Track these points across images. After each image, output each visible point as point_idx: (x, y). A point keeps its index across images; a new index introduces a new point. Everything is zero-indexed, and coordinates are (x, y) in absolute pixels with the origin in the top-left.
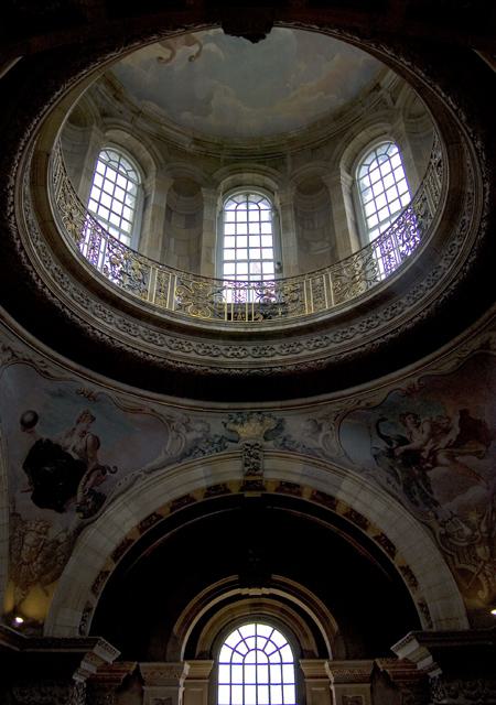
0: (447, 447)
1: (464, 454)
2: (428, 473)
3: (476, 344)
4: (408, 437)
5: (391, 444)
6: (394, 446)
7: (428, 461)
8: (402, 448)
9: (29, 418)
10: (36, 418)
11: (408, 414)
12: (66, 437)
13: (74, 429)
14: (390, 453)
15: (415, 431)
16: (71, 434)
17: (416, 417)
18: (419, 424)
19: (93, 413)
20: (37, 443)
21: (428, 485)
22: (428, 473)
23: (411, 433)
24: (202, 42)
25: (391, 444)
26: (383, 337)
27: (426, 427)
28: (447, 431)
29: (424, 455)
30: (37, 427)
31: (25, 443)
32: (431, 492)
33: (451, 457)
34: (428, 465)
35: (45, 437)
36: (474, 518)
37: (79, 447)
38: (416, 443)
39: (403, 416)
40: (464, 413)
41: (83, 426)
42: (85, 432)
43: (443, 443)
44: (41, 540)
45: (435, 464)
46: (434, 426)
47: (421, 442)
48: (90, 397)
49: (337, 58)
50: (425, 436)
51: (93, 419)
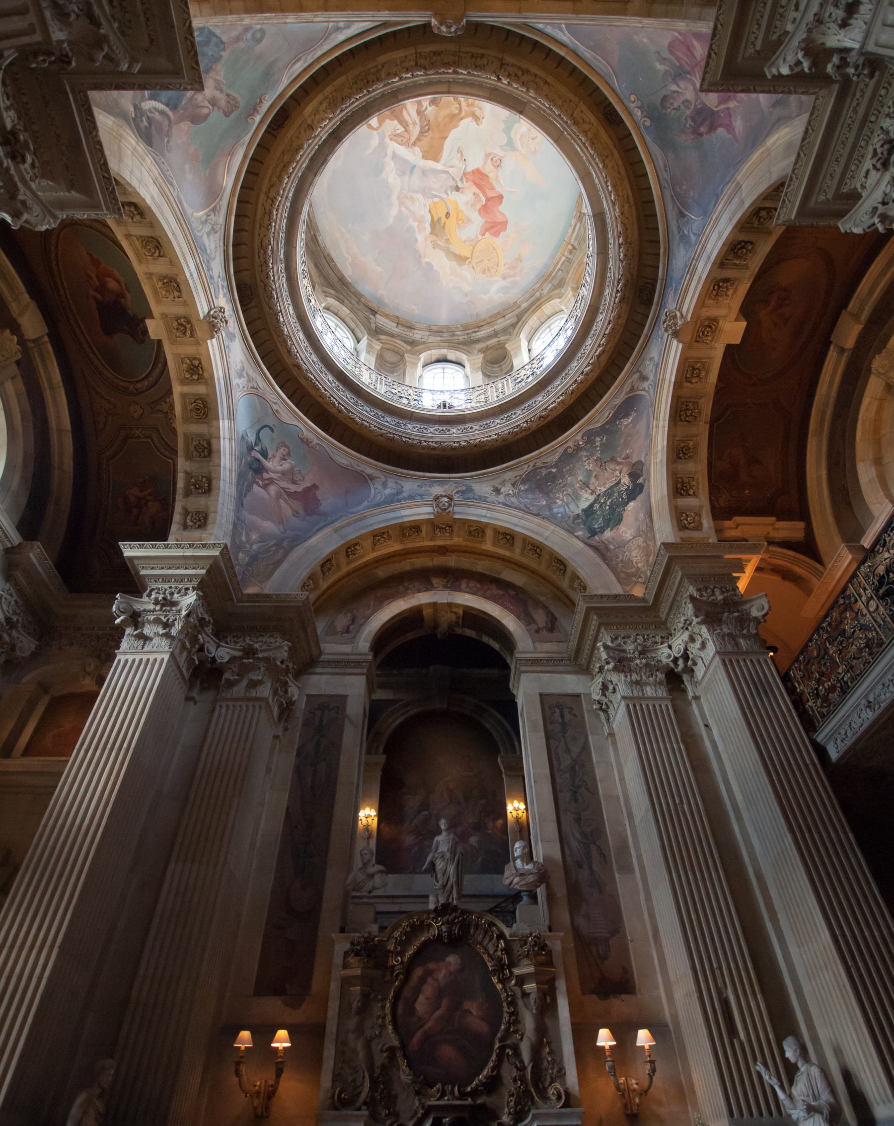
0: (283, 489)
1: (287, 502)
2: (255, 486)
3: (369, 471)
4: (270, 456)
5: (256, 444)
6: (256, 448)
7: (263, 480)
8: (259, 456)
11: (288, 448)
13: (221, 91)
14: (251, 448)
15: (277, 459)
17: (289, 454)
18: (285, 460)
21: (248, 490)
22: (255, 486)
23: (274, 456)
24: (380, 130)
25: (256, 444)
26: (339, 403)
27: (286, 466)
28: (294, 482)
29: (265, 475)
32: (245, 496)
33: (279, 496)
34: (261, 483)
36: (254, 537)
38: (268, 464)
39: (284, 445)
40: (315, 486)
43: (283, 484)
45: (265, 487)
46: (291, 471)
47: (272, 468)
49: (379, 269)
50: (279, 468)
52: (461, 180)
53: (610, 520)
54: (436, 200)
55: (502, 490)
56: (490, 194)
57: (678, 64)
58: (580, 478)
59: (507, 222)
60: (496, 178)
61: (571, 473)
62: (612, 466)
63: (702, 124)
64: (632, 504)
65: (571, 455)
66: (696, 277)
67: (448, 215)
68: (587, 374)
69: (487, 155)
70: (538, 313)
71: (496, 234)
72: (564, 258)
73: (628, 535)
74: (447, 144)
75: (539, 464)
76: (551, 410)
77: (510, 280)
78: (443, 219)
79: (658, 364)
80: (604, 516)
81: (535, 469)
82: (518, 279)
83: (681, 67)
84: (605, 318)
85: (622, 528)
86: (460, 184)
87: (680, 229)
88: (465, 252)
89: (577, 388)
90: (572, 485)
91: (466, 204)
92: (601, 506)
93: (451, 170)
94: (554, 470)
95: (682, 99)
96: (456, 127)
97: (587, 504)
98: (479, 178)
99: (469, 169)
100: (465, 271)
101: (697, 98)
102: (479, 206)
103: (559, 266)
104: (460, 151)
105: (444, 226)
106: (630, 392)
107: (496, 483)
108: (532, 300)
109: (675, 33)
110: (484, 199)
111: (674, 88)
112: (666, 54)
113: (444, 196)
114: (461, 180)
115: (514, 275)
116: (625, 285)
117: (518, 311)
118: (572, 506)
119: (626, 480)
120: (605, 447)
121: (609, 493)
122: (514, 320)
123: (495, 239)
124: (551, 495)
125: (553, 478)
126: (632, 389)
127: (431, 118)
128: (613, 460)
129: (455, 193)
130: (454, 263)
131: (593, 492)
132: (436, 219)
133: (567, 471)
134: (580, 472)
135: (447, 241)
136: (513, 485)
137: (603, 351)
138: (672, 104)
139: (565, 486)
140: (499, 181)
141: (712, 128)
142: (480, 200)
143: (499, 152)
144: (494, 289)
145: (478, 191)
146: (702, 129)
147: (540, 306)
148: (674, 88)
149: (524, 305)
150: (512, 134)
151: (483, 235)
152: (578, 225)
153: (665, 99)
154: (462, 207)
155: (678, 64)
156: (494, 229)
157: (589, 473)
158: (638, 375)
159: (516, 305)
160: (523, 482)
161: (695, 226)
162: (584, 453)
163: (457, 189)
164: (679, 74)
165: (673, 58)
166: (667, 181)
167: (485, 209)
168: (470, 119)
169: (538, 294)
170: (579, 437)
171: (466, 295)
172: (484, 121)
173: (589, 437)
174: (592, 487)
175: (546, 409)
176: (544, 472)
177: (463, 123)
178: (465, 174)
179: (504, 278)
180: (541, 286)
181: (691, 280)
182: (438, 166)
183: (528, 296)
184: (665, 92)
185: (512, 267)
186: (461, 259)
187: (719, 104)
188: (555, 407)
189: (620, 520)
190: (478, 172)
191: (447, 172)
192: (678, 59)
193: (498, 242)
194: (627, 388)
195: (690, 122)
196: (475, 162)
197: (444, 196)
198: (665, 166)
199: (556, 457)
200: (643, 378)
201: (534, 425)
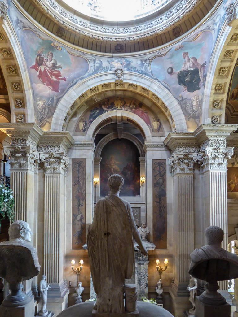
9: (170, 70)
10: (172, 69)
12: (185, 66)
16: (185, 64)
19: (186, 51)
20: (178, 75)
30: (174, 71)
31: (175, 77)
35: (179, 71)
37: (191, 65)
41: (186, 58)
42: (189, 59)
44: (198, 101)
48: (180, 48)
51: (188, 53)
57: (55, 69)
83: (54, 69)
95: (49, 61)
101: (46, 65)
109: (61, 78)
111: (52, 62)
112: (60, 69)
138: (50, 56)
148: (52, 62)
153: (52, 55)
155: (55, 69)
164: (54, 66)
165: (57, 70)
166: (36, 31)
184: (53, 58)
187: (40, 70)
192: (57, 71)
195: (43, 56)
198: (40, 36)
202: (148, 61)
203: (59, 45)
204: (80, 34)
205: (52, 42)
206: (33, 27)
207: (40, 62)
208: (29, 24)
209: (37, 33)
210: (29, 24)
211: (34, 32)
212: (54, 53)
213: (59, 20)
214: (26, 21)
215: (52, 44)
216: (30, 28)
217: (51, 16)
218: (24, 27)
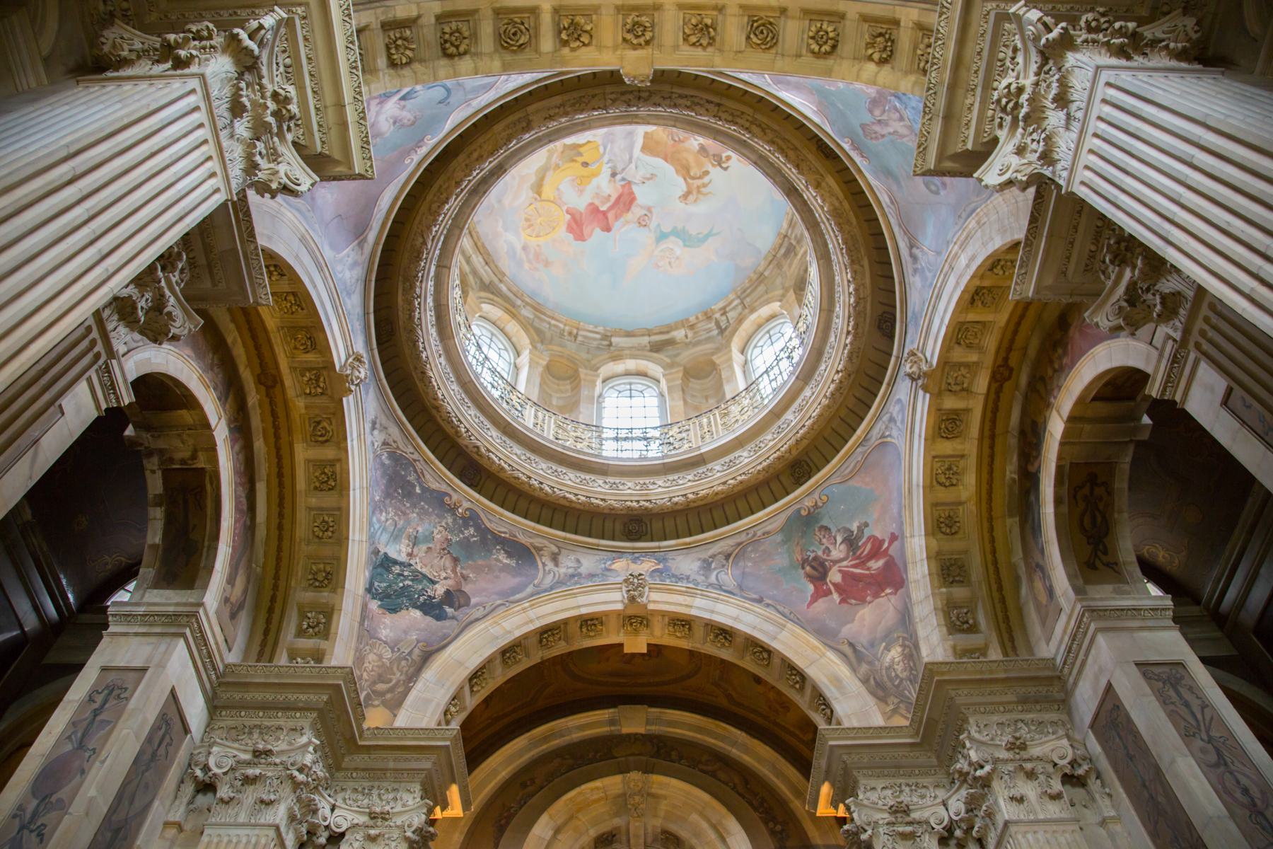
52: (623, 179)
53: (388, 596)
54: (601, 149)
55: (376, 432)
56: (611, 215)
58: (420, 529)
59: (584, 240)
60: (628, 222)
61: (423, 514)
62: (447, 562)
63: (813, 568)
64: (417, 614)
65: (442, 504)
66: (688, 600)
67: (585, 164)
68: (541, 489)
69: (649, 209)
70: (507, 317)
71: (570, 229)
72: (561, 326)
73: (384, 633)
74: (659, 162)
75: (419, 466)
76: (489, 458)
77: (523, 256)
78: (580, 159)
79: (580, 575)
80: (390, 586)
81: (411, 464)
82: (526, 266)
84: (606, 494)
85: (388, 619)
86: (618, 177)
87: (713, 556)
88: (548, 191)
89: (523, 483)
90: (408, 522)
91: (598, 187)
92: (399, 575)
93: (633, 166)
94: (418, 490)
96: (677, 172)
97: (393, 555)
98: (625, 201)
99: (635, 189)
100: (526, 194)
102: (597, 202)
103: (553, 322)
104: (653, 176)
105: (573, 161)
106: (535, 548)
107: (383, 419)
108: (511, 295)
110: (604, 208)
113: (606, 158)
114: (623, 179)
115: (529, 262)
116: (646, 509)
117: (496, 280)
118: (385, 537)
119: (440, 590)
120: (466, 545)
121: (418, 577)
122: (487, 282)
123: (563, 228)
124: (388, 501)
125: (409, 494)
126: (539, 549)
127: (686, 145)
128: (456, 560)
129: (609, 172)
130: (533, 179)
131: (410, 555)
132: (582, 150)
133: (423, 508)
134: (427, 525)
135: (557, 167)
136: (385, 443)
137: (571, 501)
139: (404, 513)
140: (624, 225)
141: (811, 578)
142: (603, 203)
143: (653, 225)
144: (510, 237)
145: (613, 199)
146: (808, 568)
147: (514, 316)
149: (503, 288)
150: (672, 238)
151: (568, 212)
152: (598, 336)
154: (595, 181)
156: (574, 226)
157: (429, 538)
158: (556, 550)
159: (501, 275)
160: (392, 455)
161: (722, 576)
162: (450, 520)
163: (614, 175)
166: (754, 535)
167: (594, 210)
168: (685, 189)
169: (519, 302)
170: (466, 505)
171: (499, 201)
172: (682, 205)
173: (470, 518)
174: (416, 550)
175: (488, 450)
176: (412, 478)
177: (681, 180)
178: (629, 183)
179: (525, 248)
180: (527, 304)
181: (681, 593)
182: (637, 151)
183: (514, 289)
185: (537, 256)
186: (538, 188)
188: (494, 462)
189: (394, 610)
190: (632, 199)
191: (630, 161)
193: (562, 233)
194: (538, 542)
195: (812, 555)
196: (643, 195)
197: (606, 158)
198: (768, 533)
199: (434, 485)
200: (555, 558)
201: (466, 442)
202: (915, 251)
203: (816, 496)
204: (812, 428)
205: (799, 510)
206: (743, 537)
207: (818, 571)
208: (731, 542)
209: (759, 533)
210: (731, 542)
211: (755, 542)
212: (824, 523)
213: (759, 468)
214: (722, 543)
215: (804, 513)
216: (739, 544)
217: (741, 482)
218: (728, 557)
